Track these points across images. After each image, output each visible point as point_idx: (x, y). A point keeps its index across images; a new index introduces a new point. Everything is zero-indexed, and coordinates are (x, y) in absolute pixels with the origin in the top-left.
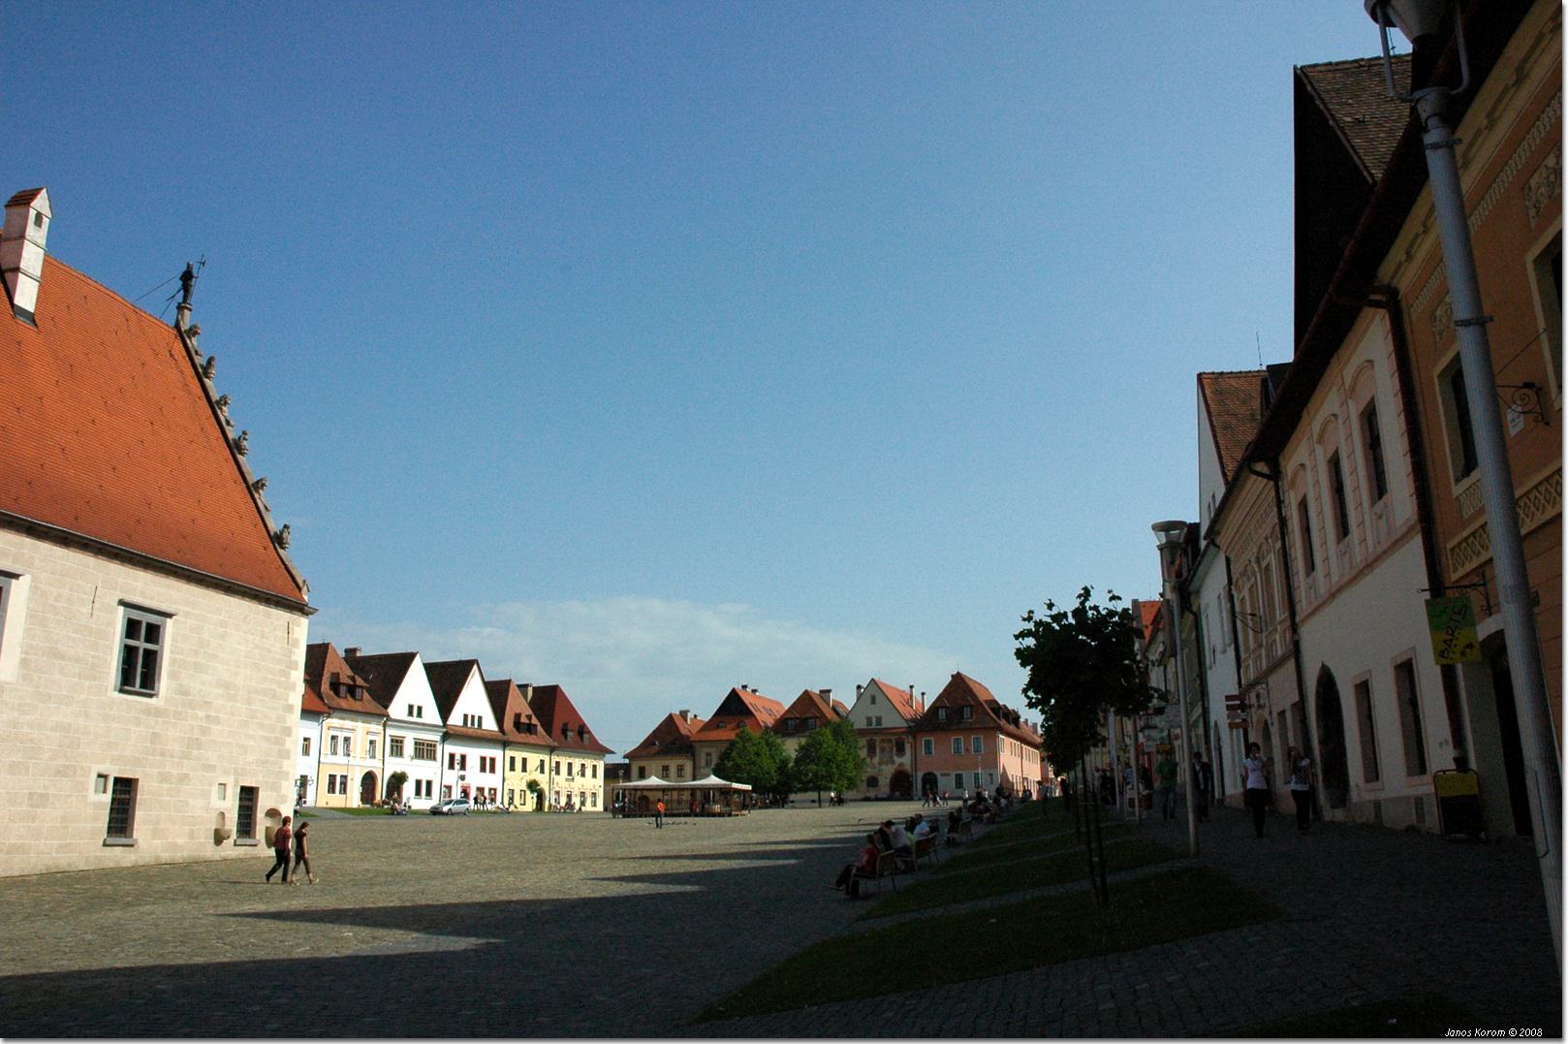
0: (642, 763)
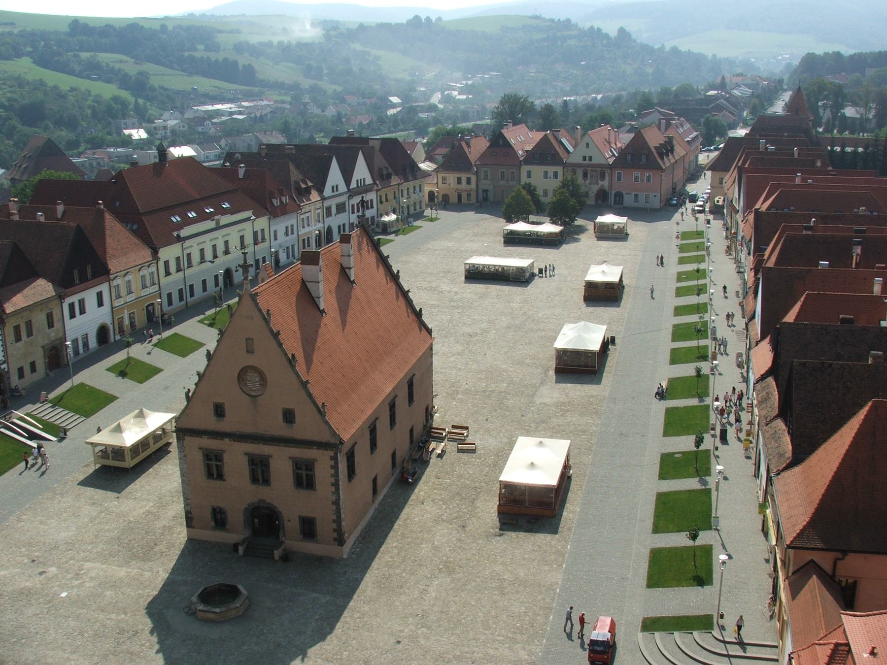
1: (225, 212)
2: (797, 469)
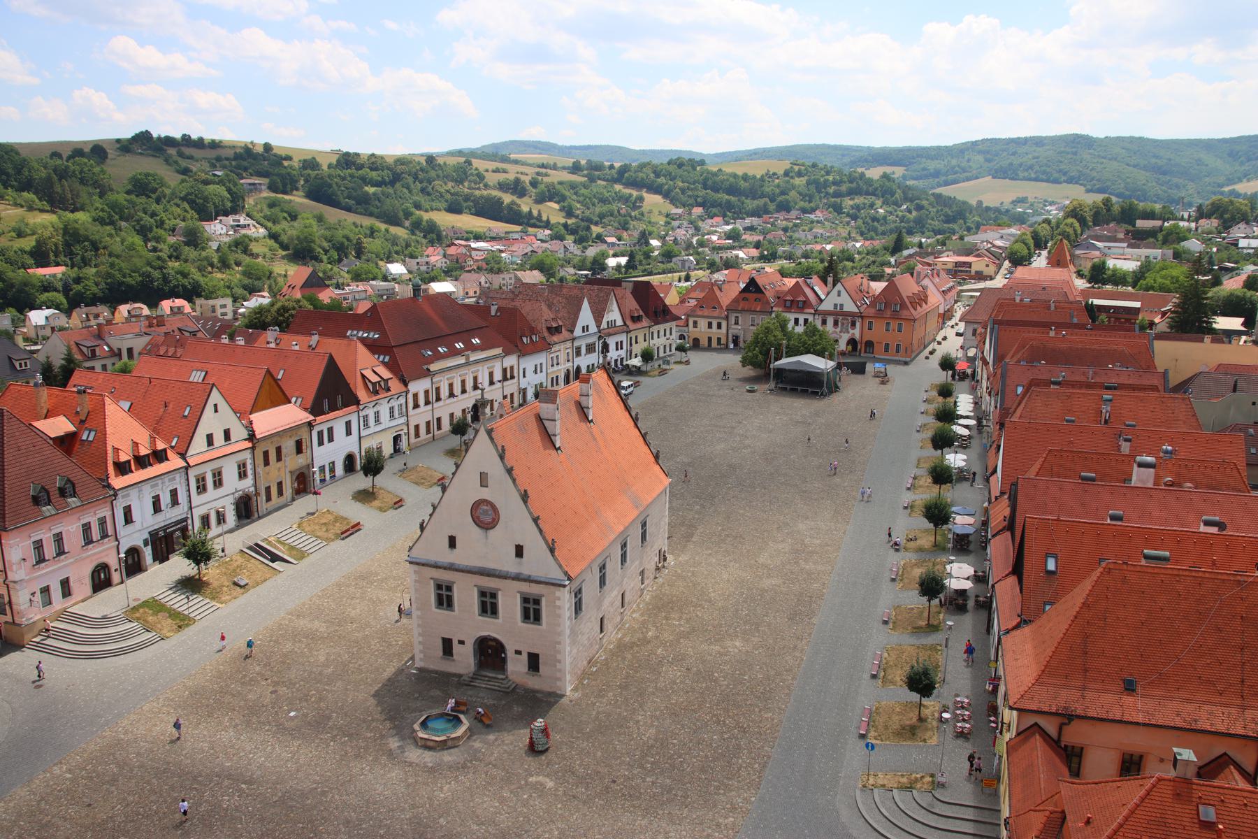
0: (696, 319)
1: (475, 348)
2: (1026, 630)
